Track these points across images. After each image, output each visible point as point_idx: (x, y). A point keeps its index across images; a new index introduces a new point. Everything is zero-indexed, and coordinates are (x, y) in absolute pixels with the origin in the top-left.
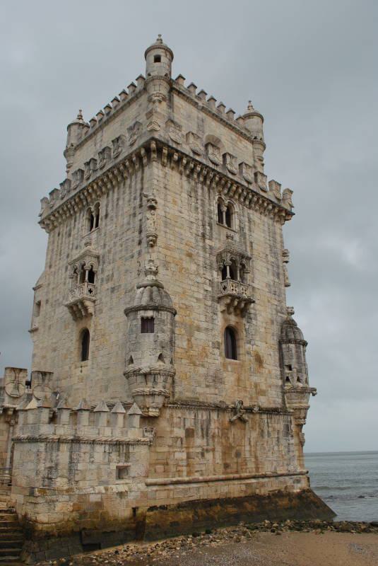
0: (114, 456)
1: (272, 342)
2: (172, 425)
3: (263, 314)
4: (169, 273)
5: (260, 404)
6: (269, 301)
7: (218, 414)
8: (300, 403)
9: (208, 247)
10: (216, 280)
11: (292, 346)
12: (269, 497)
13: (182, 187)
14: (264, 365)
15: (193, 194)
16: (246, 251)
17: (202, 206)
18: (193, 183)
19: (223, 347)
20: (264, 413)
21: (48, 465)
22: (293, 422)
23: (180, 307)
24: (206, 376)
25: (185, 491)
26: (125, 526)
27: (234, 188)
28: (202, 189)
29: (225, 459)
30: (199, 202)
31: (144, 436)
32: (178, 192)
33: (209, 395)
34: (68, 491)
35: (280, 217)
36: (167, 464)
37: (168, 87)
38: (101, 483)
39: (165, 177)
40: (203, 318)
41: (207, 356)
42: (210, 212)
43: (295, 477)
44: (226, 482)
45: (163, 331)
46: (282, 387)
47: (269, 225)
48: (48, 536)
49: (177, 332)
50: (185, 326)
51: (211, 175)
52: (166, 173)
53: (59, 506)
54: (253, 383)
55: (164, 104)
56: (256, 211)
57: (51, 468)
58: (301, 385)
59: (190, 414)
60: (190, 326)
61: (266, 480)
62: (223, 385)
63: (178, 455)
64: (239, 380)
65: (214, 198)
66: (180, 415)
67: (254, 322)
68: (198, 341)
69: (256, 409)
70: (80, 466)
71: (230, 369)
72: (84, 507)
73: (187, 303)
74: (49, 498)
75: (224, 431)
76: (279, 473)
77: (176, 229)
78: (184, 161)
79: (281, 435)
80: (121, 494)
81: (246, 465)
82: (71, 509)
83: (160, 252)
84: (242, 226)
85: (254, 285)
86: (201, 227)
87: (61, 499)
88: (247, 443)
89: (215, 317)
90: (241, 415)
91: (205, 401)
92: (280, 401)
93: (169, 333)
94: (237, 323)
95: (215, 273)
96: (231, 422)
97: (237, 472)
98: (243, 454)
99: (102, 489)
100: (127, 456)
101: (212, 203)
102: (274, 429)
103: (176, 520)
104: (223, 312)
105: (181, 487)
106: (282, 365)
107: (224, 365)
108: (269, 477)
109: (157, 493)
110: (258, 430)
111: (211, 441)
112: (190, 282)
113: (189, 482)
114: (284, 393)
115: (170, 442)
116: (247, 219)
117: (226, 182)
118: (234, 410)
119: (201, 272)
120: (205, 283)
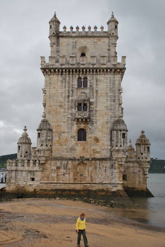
0: (29, 174)
1: (106, 131)
2: (51, 165)
3: (101, 120)
4: (51, 115)
5: (96, 157)
6: (106, 114)
7: (72, 162)
8: (118, 155)
9: (70, 100)
10: (74, 112)
11: (115, 132)
12: (96, 191)
13: (58, 80)
14: (100, 141)
15: (64, 81)
16: (93, 95)
17: (68, 84)
18: (64, 76)
19: (77, 137)
20: (97, 160)
21: (9, 176)
22: (116, 163)
23: (55, 126)
24: (67, 149)
25: (55, 186)
26: (32, 194)
27: (84, 70)
28: (69, 77)
29: (75, 177)
30: (67, 83)
31: (40, 169)
32: (57, 83)
33: (69, 155)
34: (14, 183)
35: (117, 72)
36: (49, 177)
37: (56, 38)
38: (25, 182)
39: (50, 79)
40: (66, 128)
41: (68, 142)
42: (72, 85)
43: (113, 185)
44: (75, 184)
45: (43, 137)
46: (111, 149)
47: (110, 78)
48: (9, 193)
49: (54, 135)
50: (58, 132)
51: (71, 70)
52: (51, 78)
53: (11, 187)
54: (92, 149)
55: (55, 46)
56: (102, 74)
57: (10, 177)
58: (117, 148)
59: (59, 162)
60: (60, 132)
61: (96, 185)
62: (75, 151)
63: (53, 175)
64: (84, 149)
65: (75, 78)
66: (54, 162)
67: (95, 125)
68: (63, 137)
69: (90, 159)
70: (18, 177)
71: (79, 145)
72: (19, 188)
73: (59, 124)
74: (9, 184)
75: (75, 167)
76: (103, 183)
77: (55, 98)
78: (57, 70)
79: (107, 169)
80: (30, 185)
81: (86, 179)
82: (15, 188)
83: (47, 109)
84: (91, 84)
85: (96, 109)
86: (67, 93)
87: (12, 185)
88: (87, 171)
89: (73, 126)
90: (82, 161)
91: (66, 157)
92: (109, 155)
93: (45, 137)
94: (85, 127)
95: (74, 110)
96: (79, 164)
97: (80, 181)
98: (84, 175)
99: (25, 183)
100: (34, 175)
101: (74, 81)
102: (103, 166)
103: (48, 193)
104: (76, 124)
105: (53, 184)
106: (111, 140)
107: (77, 144)
108: (98, 184)
109: (43, 186)
110: (93, 167)
111: (68, 171)
112: (61, 116)
113: (56, 183)
114: (111, 152)
115: (50, 171)
116: (95, 81)
117: (80, 70)
118: (79, 160)
119: (66, 111)
120: (68, 115)
